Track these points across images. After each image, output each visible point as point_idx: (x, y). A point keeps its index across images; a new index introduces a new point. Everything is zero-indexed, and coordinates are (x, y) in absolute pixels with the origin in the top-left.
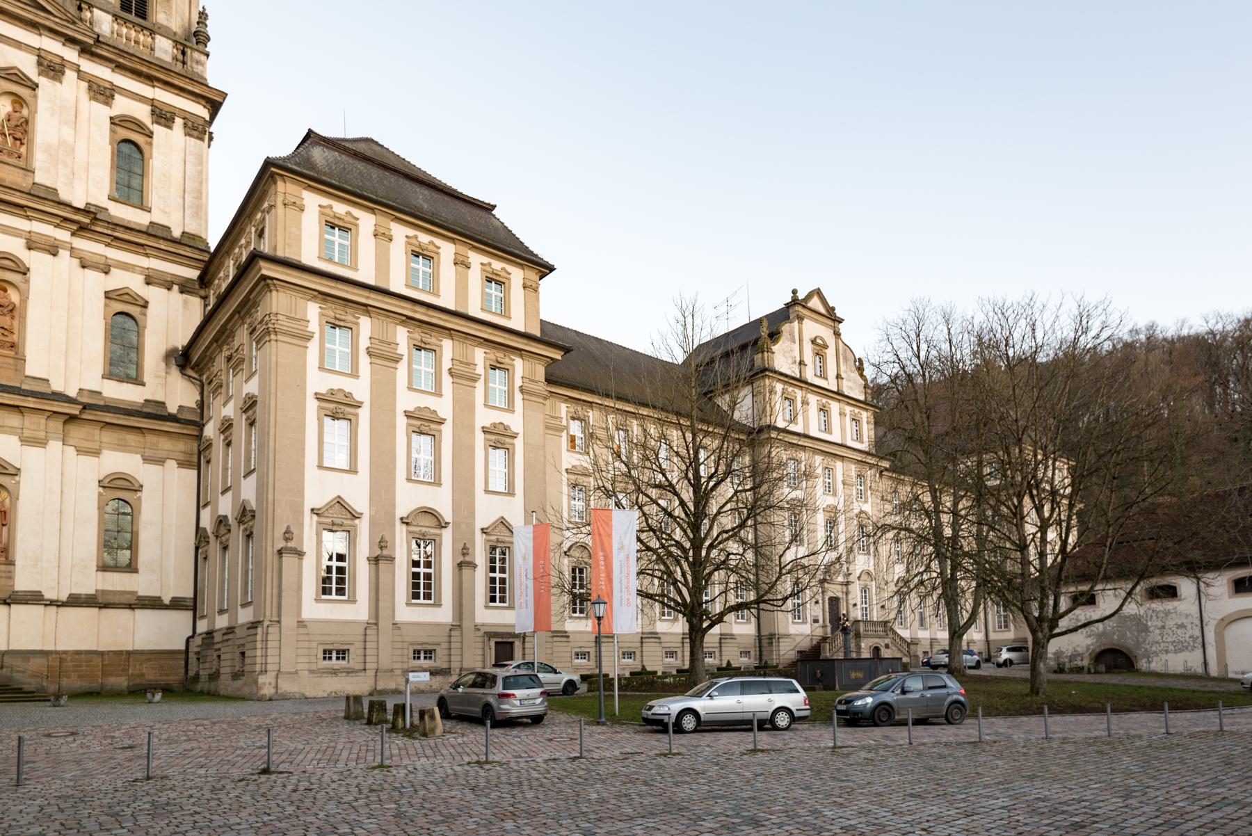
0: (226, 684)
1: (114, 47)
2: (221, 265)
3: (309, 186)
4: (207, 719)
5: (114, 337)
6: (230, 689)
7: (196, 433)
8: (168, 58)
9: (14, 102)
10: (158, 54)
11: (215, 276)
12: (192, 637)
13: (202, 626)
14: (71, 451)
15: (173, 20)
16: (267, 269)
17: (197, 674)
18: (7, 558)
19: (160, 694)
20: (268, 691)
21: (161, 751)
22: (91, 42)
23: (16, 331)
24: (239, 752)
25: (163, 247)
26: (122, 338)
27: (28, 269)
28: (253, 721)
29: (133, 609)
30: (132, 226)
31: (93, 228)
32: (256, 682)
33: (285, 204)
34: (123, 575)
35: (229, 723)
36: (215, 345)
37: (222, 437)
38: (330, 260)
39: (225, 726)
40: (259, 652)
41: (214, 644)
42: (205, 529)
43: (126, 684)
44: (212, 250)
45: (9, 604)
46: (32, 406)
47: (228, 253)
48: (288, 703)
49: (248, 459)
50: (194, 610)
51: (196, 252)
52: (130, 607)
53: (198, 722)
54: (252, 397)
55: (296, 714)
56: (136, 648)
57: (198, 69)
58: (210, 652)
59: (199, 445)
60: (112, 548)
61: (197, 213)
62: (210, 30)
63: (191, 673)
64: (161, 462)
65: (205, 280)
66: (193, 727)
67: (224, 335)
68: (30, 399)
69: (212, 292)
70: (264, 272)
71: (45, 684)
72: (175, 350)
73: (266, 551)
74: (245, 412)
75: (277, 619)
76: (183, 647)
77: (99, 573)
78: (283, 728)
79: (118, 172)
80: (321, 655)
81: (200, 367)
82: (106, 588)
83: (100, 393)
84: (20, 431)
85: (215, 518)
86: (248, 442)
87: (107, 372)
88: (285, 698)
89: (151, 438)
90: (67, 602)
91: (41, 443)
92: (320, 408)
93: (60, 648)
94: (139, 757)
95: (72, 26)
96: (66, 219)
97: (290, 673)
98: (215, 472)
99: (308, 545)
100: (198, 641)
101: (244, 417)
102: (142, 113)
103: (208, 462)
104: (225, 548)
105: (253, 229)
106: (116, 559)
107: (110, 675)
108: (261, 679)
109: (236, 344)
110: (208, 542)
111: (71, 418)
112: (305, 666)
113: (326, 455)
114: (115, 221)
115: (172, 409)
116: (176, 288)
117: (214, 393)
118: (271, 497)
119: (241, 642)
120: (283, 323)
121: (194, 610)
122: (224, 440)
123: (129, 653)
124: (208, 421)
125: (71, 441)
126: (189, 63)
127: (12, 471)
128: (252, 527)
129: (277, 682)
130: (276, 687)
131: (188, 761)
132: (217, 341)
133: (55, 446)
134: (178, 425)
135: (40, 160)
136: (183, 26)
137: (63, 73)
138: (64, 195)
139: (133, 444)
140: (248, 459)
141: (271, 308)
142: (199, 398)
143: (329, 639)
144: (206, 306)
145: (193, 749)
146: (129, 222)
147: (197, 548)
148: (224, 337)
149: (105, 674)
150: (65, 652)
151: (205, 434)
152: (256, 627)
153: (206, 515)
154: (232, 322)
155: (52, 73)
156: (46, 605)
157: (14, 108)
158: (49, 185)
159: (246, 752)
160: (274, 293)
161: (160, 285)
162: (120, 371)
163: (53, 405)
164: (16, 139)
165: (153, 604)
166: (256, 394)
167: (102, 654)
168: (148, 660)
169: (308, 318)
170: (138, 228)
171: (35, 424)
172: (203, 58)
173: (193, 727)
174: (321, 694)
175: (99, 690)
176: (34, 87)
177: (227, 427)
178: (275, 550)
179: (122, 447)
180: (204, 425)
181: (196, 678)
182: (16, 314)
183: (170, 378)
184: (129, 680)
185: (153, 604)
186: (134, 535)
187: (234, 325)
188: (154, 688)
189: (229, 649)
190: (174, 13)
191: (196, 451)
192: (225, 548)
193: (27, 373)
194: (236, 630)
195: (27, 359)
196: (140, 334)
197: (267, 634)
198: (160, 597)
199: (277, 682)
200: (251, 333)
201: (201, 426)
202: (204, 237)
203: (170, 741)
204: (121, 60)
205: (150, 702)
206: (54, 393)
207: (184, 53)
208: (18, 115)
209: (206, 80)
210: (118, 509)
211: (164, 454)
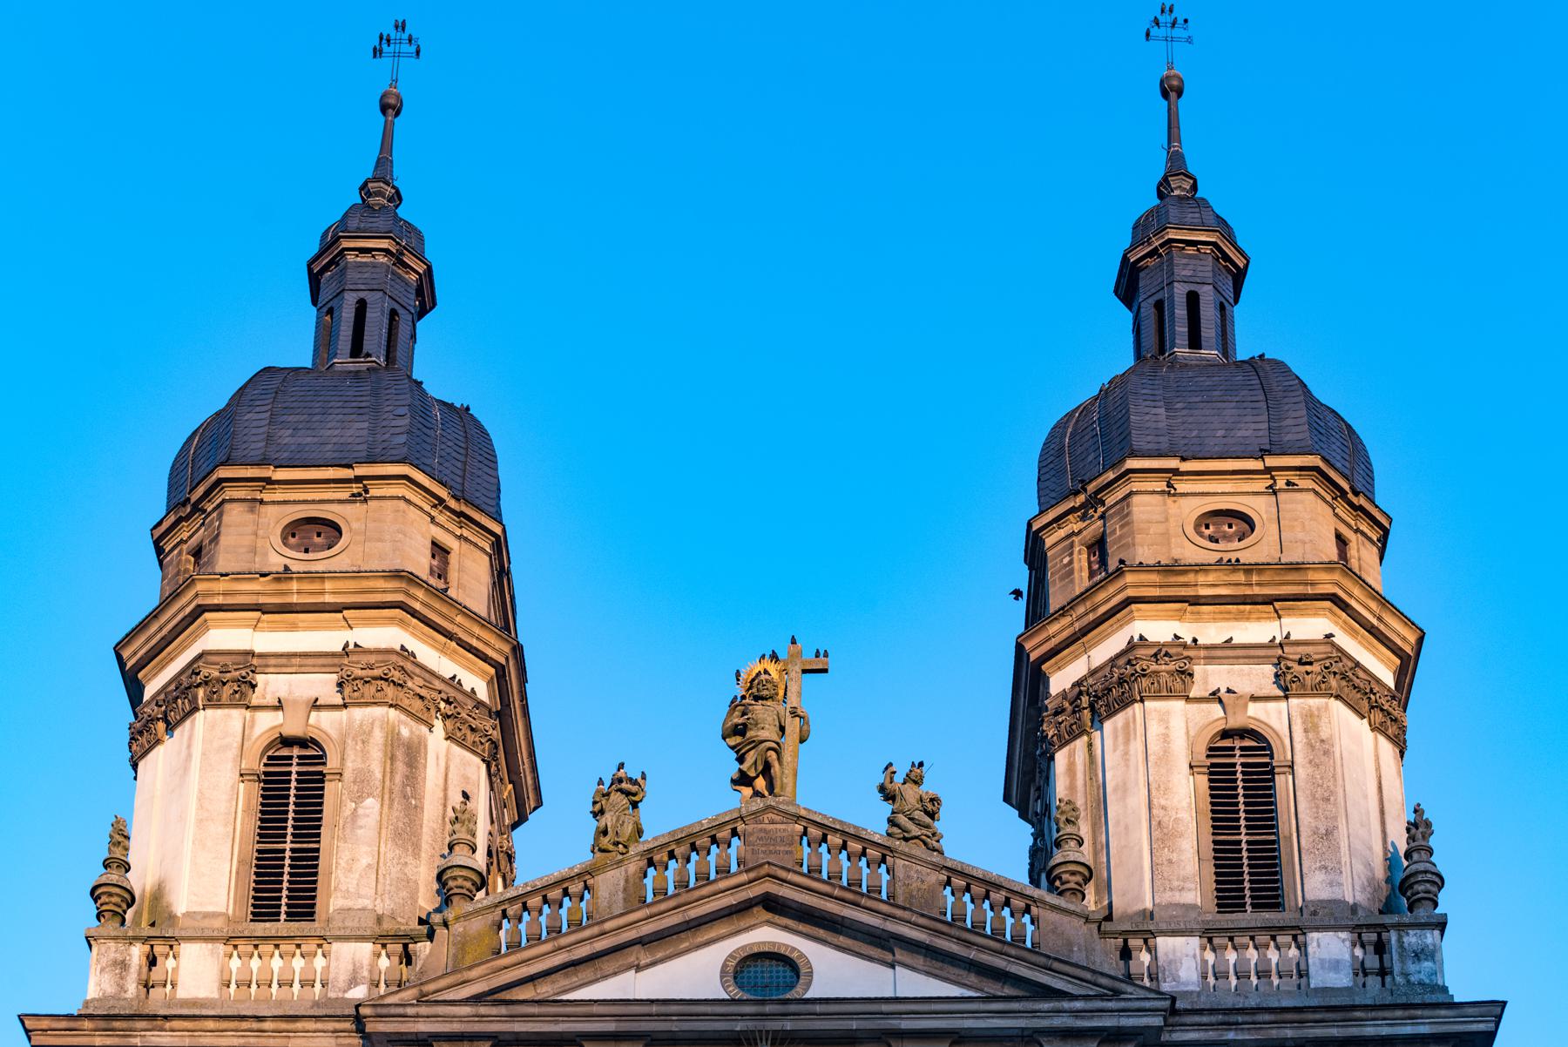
1: (1212, 1011)
8: (1343, 979)
15: (1346, 879)
22: (1157, 1021)
62: (1441, 861)
95: (1111, 1005)
126: (1397, 968)
136: (1371, 880)
172: (1431, 937)
190: (1345, 859)
207: (1380, 948)
209: (1445, 989)
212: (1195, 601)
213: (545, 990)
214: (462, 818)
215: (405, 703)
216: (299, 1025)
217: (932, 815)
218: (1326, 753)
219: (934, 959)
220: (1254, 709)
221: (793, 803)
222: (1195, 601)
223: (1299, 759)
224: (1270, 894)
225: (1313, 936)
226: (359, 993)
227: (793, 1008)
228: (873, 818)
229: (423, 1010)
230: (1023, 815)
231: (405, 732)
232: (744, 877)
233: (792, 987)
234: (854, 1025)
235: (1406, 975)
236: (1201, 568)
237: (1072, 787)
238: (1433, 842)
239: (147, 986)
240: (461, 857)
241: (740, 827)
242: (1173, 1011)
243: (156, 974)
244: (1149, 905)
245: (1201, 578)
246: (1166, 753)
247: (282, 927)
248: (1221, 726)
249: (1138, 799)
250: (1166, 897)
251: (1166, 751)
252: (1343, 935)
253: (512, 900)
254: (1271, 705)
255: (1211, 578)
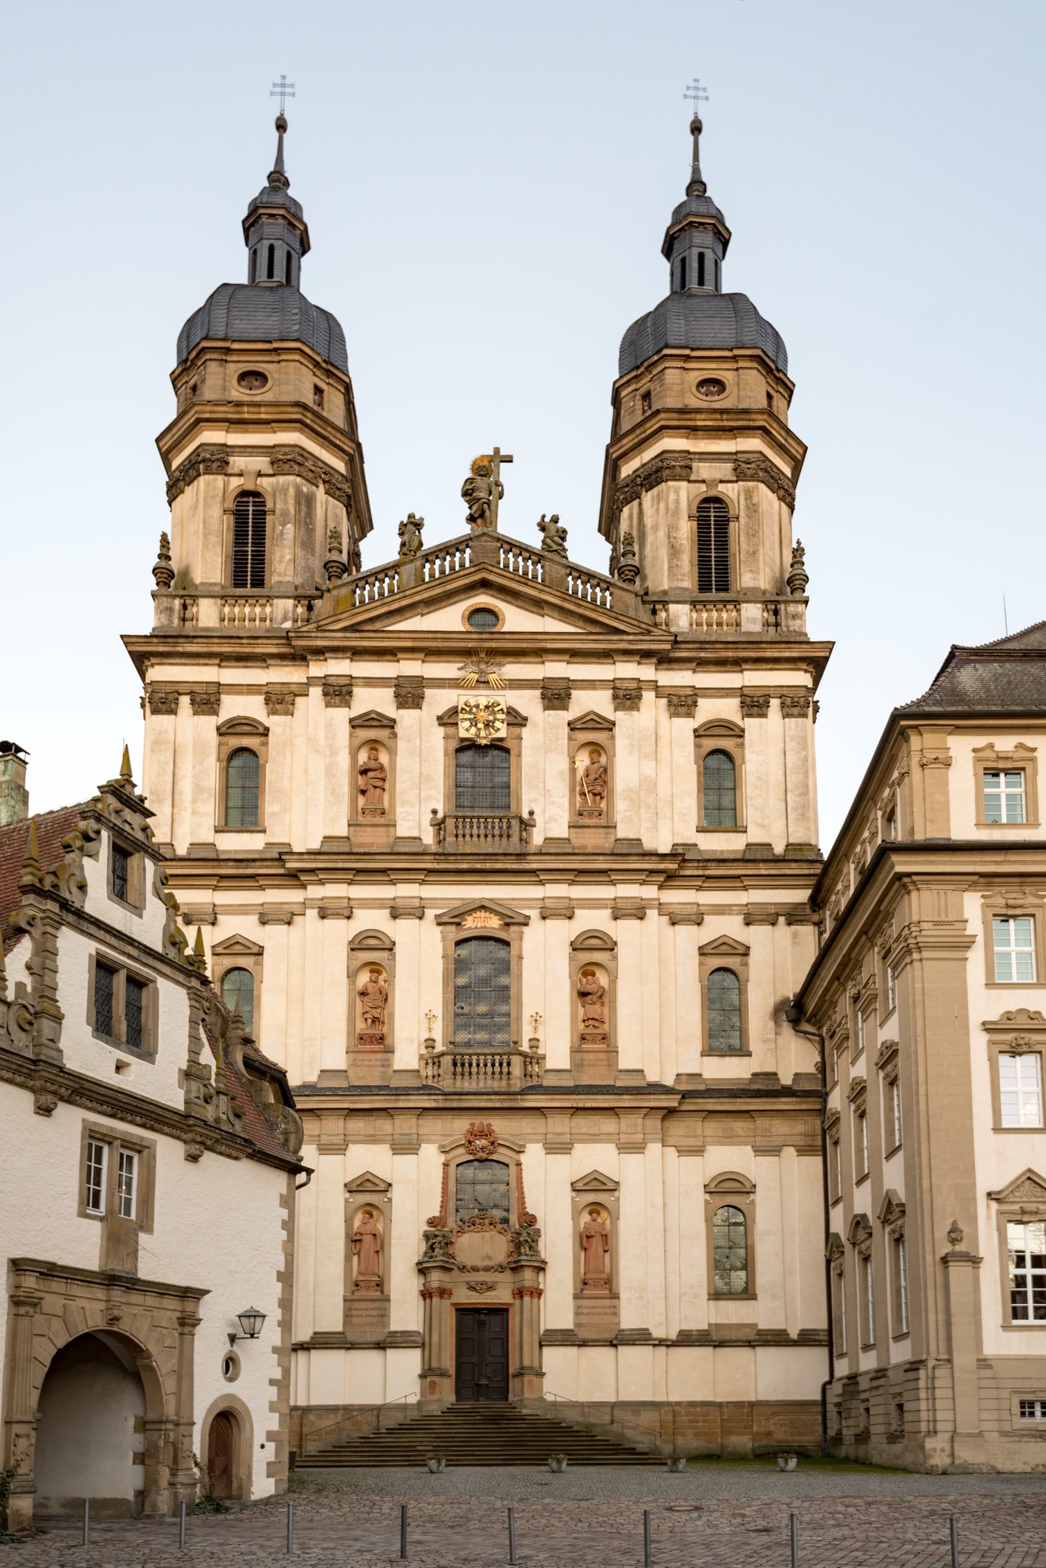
0: (878, 1448)
1: (694, 642)
2: (839, 872)
3: (957, 727)
4: (859, 1497)
5: (712, 1001)
6: (885, 1455)
7: (818, 1107)
8: (757, 628)
9: (591, 753)
10: (746, 627)
11: (830, 890)
12: (830, 1382)
13: (842, 1368)
14: (671, 1152)
15: (761, 577)
16: (901, 864)
17: (839, 1433)
18: (611, 1291)
19: (795, 1460)
20: (940, 1460)
21: (804, 1537)
22: (668, 647)
23: (606, 1020)
24: (908, 1547)
25: (763, 872)
26: (721, 999)
27: (616, 943)
28: (924, 1504)
29: (753, 1347)
30: (726, 856)
31: (682, 873)
32: (922, 1447)
33: (923, 766)
34: (738, 1303)
35: (889, 1504)
36: (836, 983)
37: (853, 1107)
38: (996, 824)
39: (884, 1509)
40: (923, 1405)
41: (859, 1392)
42: (837, 1235)
43: (750, 1445)
44: (826, 857)
45: (615, 1346)
46: (627, 1105)
47: (847, 856)
48: (971, 1480)
49: (890, 1132)
50: (830, 1346)
51: (805, 865)
52: (750, 1344)
53: (847, 1501)
54: (891, 1046)
55: (986, 1496)
56: (759, 1398)
57: (795, 625)
58: (855, 1404)
59: (823, 1122)
60: (725, 1269)
61: (803, 815)
62: (808, 569)
63: (831, 1433)
64: (775, 1151)
65: (817, 902)
66: (841, 1508)
67: (850, 966)
68: (625, 1097)
69: (828, 913)
70: (899, 869)
71: (658, 1443)
72: (785, 1002)
73: (924, 1259)
74: (882, 1067)
75: (946, 1357)
76: (818, 1397)
77: (711, 1302)
78: (968, 1516)
79: (706, 795)
80: (1017, 1410)
81: (817, 1019)
82: (719, 1322)
83: (700, 1075)
84: (616, 1137)
85: (850, 1219)
86: (890, 1109)
87: (706, 1047)
88: (966, 1471)
89: (762, 1122)
90: (677, 1341)
91: (637, 1148)
92: (991, 1043)
93: (673, 1398)
94: (778, 1544)
95: (646, 638)
96: (652, 872)
97: (970, 1435)
98: (846, 1157)
99: (987, 1246)
100: (837, 1388)
101: (881, 1074)
102: (729, 709)
103: (836, 1143)
104: (866, 1259)
105: (880, 813)
106: (728, 1284)
107: (731, 1433)
108: (930, 1444)
109: (865, 976)
110: (843, 1253)
111: (670, 1112)
112: (996, 1426)
113: (1004, 1109)
114: (706, 857)
115: (786, 1080)
116: (782, 920)
117: (838, 1049)
118: (926, 1184)
119: (897, 1389)
120: (929, 933)
121: (830, 1346)
122: (855, 1111)
123: (752, 1405)
124: (832, 1089)
125: (671, 1141)
126: (783, 623)
127: (611, 1186)
128: (902, 1227)
129: (952, 1447)
130: (952, 1455)
131: (840, 1555)
132: (838, 979)
133: (654, 1149)
134: (795, 1099)
135: (621, 809)
137: (639, 697)
138: (648, 845)
139: (741, 1133)
140: (890, 1132)
141: (911, 917)
142: (819, 1059)
143: (1028, 1385)
144: (821, 933)
145: (845, 1539)
146: (722, 852)
147: (828, 1262)
148: (847, 971)
149: (726, 1432)
150: (678, 1404)
151: (829, 1107)
152: (918, 1369)
153: (838, 1215)
154: (858, 947)
155: (628, 703)
156: (654, 1345)
157: (592, 759)
158: (632, 837)
159: (918, 1548)
160: (914, 895)
161: (762, 922)
162: (721, 1043)
163: (649, 1100)
164: (595, 795)
165: (777, 1339)
166: (897, 1040)
167: (720, 1405)
168: (775, 1414)
169: (966, 917)
170: (732, 857)
171: (631, 1126)
172: (801, 607)
173: (841, 1508)
174: (1020, 1468)
175: (719, 1452)
176: (610, 726)
177: (858, 1091)
178: (938, 1257)
179: (729, 1139)
180: (827, 1094)
181: (838, 1439)
182: (606, 999)
183: (780, 1039)
184: (754, 1439)
185: (777, 1339)
186: (749, 1249)
187: (860, 952)
188: (786, 1451)
189: (881, 1400)
190: (761, 566)
191: (819, 1131)
192: (866, 1259)
193: (620, 1067)
194: (889, 1373)
195: (620, 1050)
196: (742, 992)
197: (934, 1378)
198: (785, 1330)
199: (952, 1447)
200: (884, 958)
201: (823, 1096)
202: (813, 843)
203: (816, 1526)
204: (703, 655)
205: (783, 1471)
206: (650, 1085)
207: (776, 612)
208: (596, 765)
209: (806, 635)
210: (728, 1219)
211: (777, 1141)
212: (695, 429)
213: (378, 626)
214: (335, 535)
215: (304, 474)
216: (259, 641)
217: (563, 539)
218: (755, 511)
219: (564, 613)
220: (721, 487)
221: (495, 531)
222: (695, 429)
223: (742, 514)
224: (724, 586)
225: (744, 606)
226: (288, 625)
227: (496, 636)
228: (535, 540)
229: (319, 634)
230: (608, 539)
231: (305, 489)
232: (473, 569)
233: (495, 625)
234: (525, 645)
235: (787, 626)
236: (698, 411)
237: (631, 526)
238: (805, 559)
239: (184, 620)
240: (334, 556)
241: (470, 544)
242: (676, 642)
243: (188, 615)
244: (666, 587)
245: (698, 416)
246: (677, 510)
247: (248, 590)
248: (704, 496)
249: (662, 534)
250: (675, 584)
251: (677, 508)
252: (759, 605)
253: (360, 579)
254: (730, 485)
255: (703, 416)
